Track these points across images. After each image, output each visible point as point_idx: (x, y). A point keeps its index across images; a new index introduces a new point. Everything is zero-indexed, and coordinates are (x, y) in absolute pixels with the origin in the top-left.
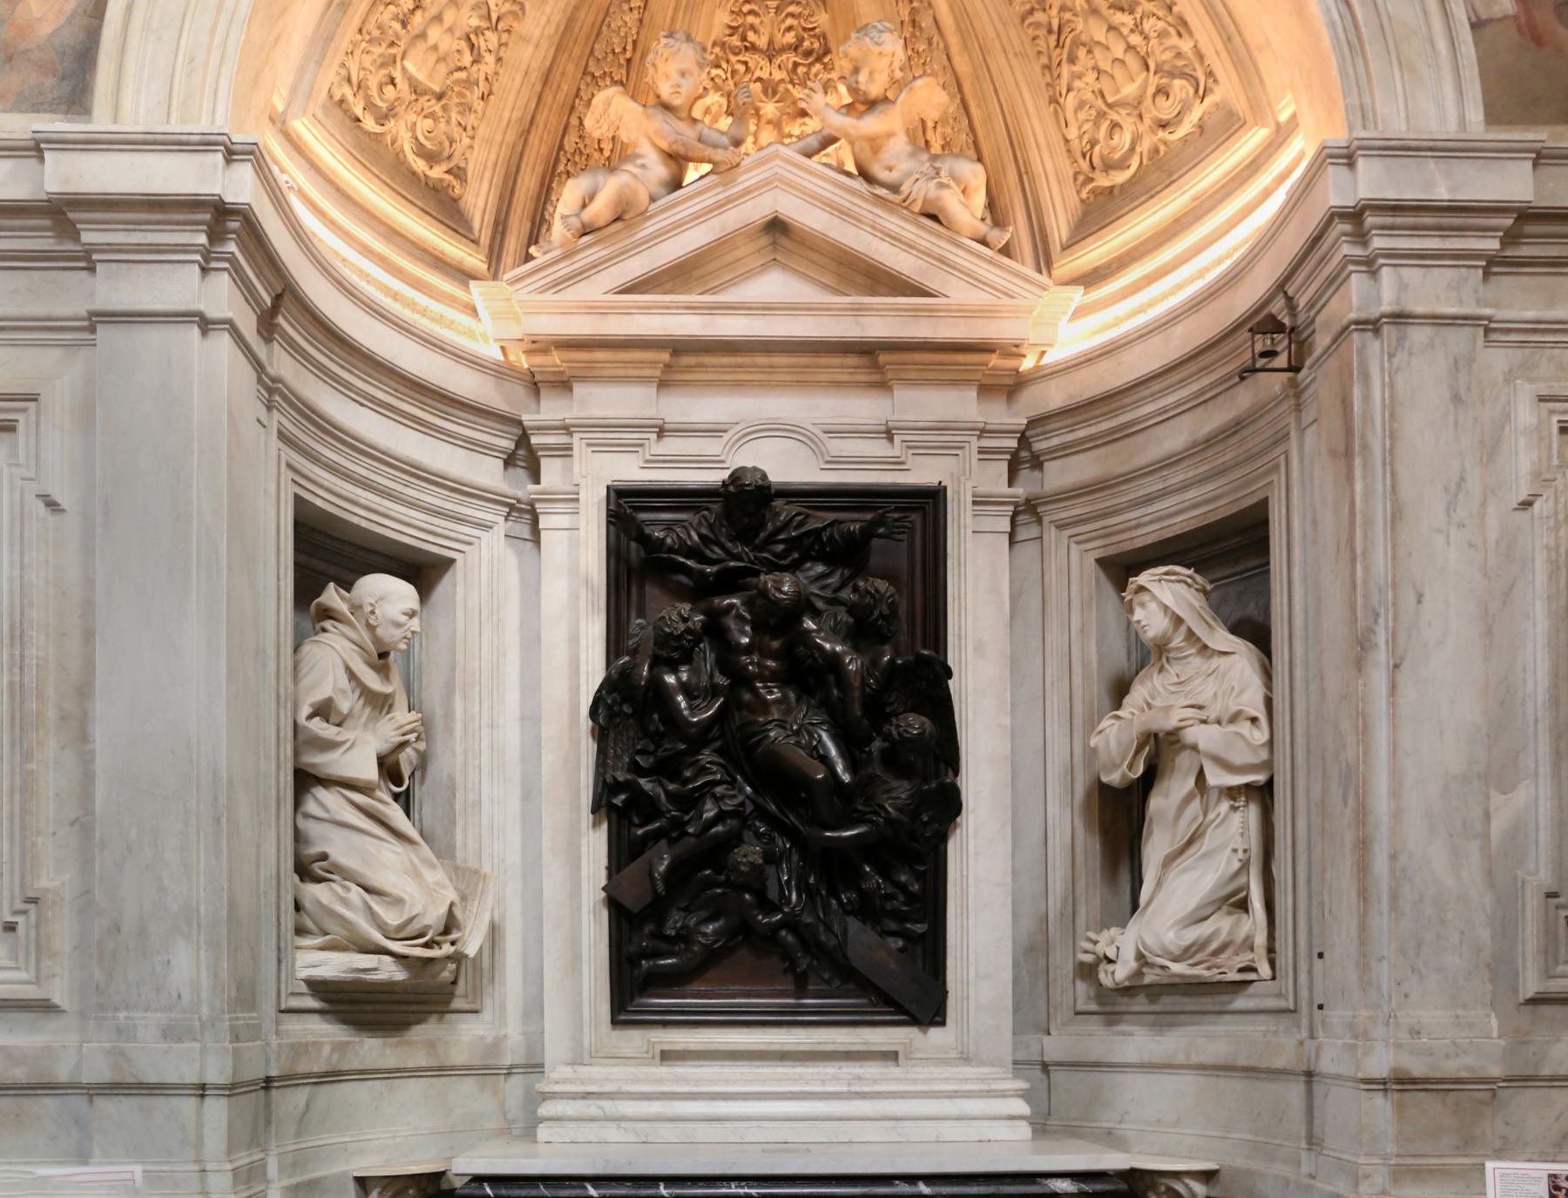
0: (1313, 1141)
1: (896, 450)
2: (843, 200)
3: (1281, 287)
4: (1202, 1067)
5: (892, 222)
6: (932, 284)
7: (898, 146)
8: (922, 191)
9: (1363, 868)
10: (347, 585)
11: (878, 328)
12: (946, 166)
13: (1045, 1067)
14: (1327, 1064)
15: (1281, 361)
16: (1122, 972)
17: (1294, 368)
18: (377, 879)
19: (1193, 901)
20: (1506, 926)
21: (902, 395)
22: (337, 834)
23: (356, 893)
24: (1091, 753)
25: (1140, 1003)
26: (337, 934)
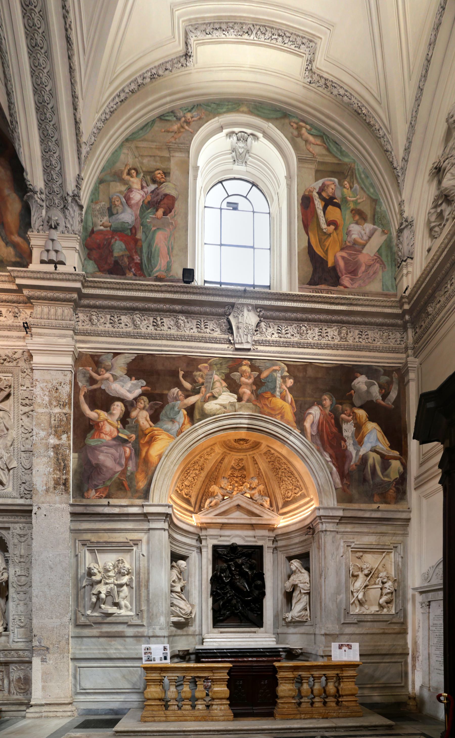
0: (315, 643)
1: (256, 540)
2: (248, 502)
3: (311, 523)
4: (301, 634)
5: (256, 506)
6: (262, 515)
7: (257, 494)
8: (260, 502)
9: (321, 605)
10: (176, 562)
11: (254, 522)
12: (264, 498)
13: (278, 634)
14: (317, 633)
15: (311, 533)
16: (289, 619)
17: (313, 534)
18: (181, 606)
19: (299, 609)
20: (339, 614)
21: (257, 531)
22: (175, 600)
23: (178, 608)
24: (285, 587)
25: (292, 624)
26: (175, 614)
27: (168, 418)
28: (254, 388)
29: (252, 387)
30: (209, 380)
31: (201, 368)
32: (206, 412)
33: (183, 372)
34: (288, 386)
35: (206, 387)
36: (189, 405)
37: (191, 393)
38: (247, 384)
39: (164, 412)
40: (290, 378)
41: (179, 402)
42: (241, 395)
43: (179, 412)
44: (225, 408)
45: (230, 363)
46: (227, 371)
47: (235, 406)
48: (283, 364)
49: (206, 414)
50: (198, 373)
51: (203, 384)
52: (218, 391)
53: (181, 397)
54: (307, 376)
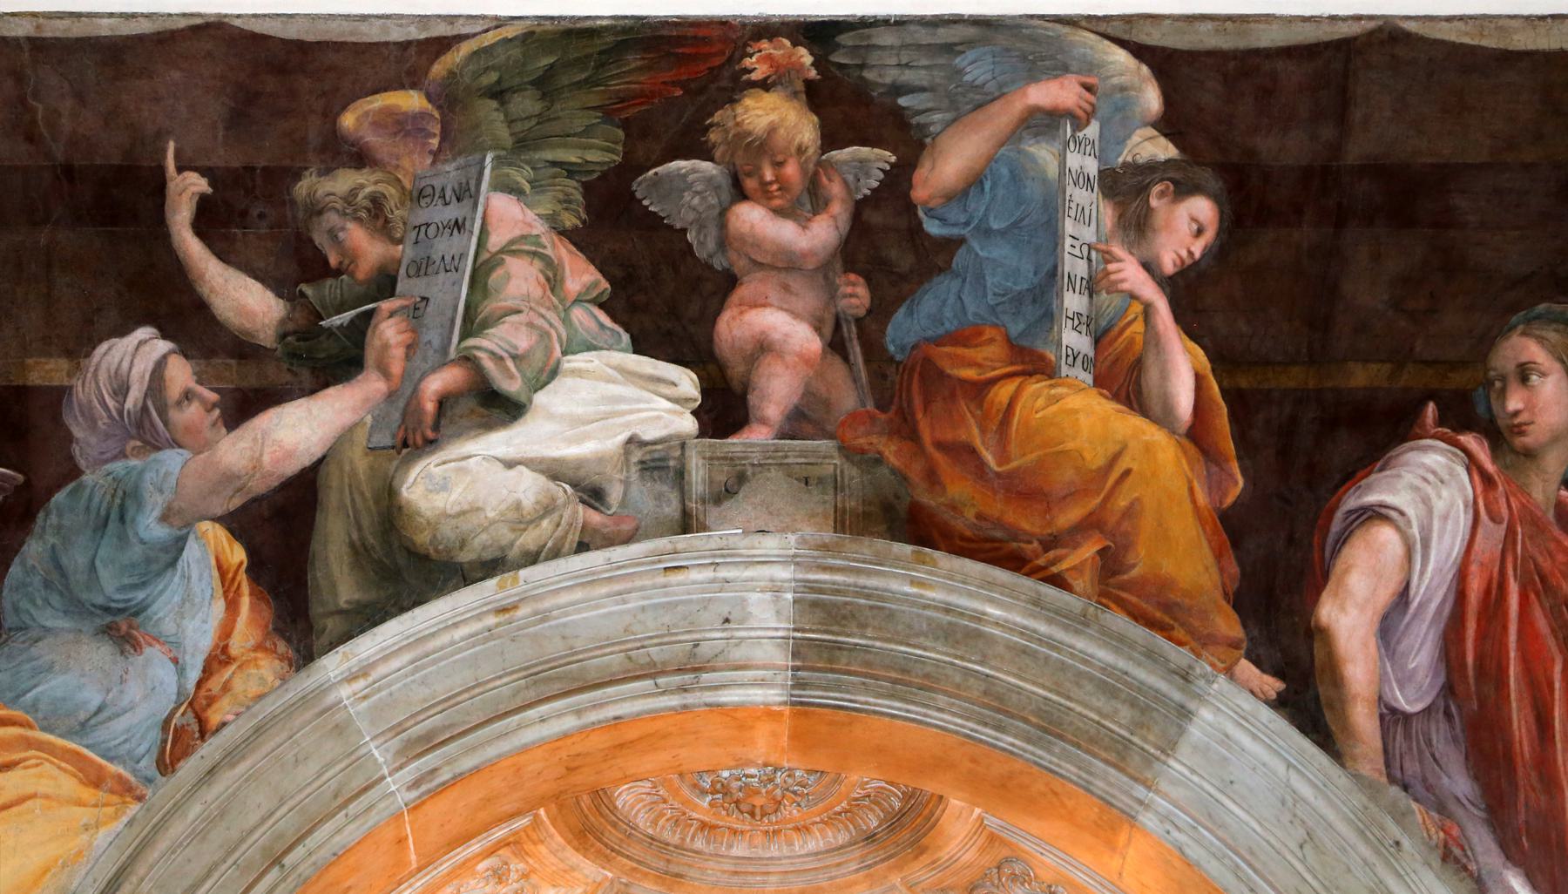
27: (76, 607)
28: (856, 295)
29: (832, 292)
30: (444, 246)
31: (371, 138)
32: (422, 539)
33: (197, 184)
34: (1169, 265)
35: (415, 312)
36: (259, 486)
37: (276, 374)
38: (786, 264)
39: (34, 549)
40: (1183, 190)
41: (172, 461)
42: (736, 369)
43: (179, 544)
44: (593, 495)
45: (631, 74)
46: (599, 154)
47: (681, 475)
48: (1121, 56)
49: (420, 559)
50: (344, 181)
51: (385, 283)
52: (523, 342)
53: (193, 411)
54: (1357, 150)
